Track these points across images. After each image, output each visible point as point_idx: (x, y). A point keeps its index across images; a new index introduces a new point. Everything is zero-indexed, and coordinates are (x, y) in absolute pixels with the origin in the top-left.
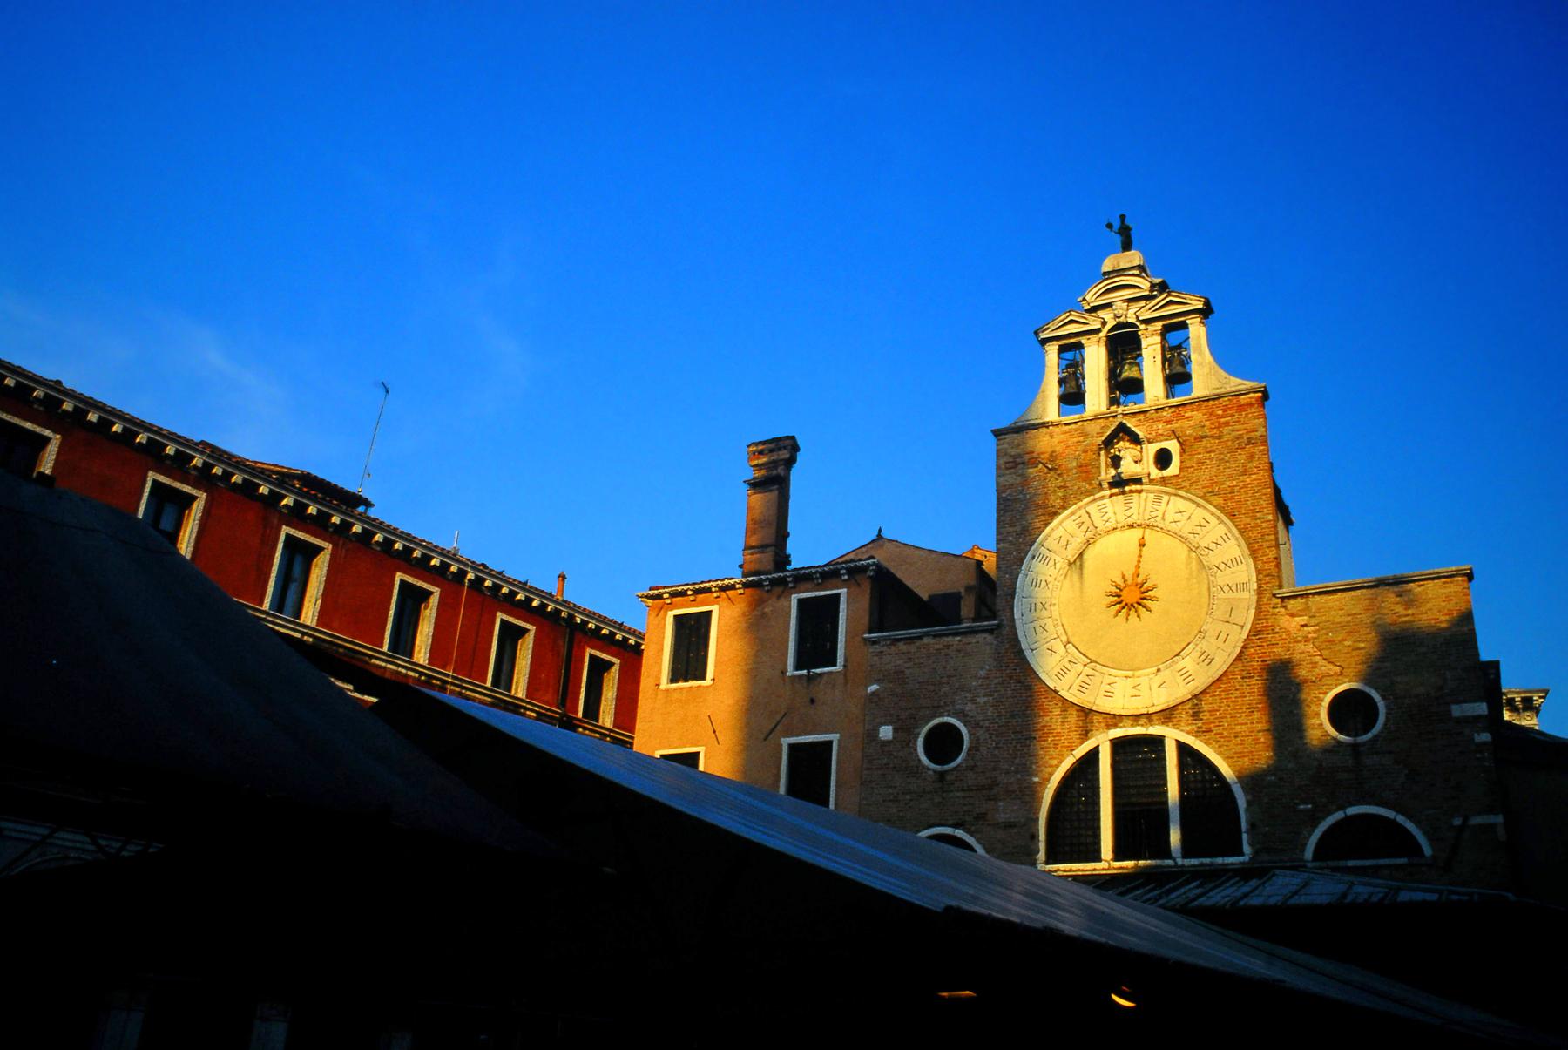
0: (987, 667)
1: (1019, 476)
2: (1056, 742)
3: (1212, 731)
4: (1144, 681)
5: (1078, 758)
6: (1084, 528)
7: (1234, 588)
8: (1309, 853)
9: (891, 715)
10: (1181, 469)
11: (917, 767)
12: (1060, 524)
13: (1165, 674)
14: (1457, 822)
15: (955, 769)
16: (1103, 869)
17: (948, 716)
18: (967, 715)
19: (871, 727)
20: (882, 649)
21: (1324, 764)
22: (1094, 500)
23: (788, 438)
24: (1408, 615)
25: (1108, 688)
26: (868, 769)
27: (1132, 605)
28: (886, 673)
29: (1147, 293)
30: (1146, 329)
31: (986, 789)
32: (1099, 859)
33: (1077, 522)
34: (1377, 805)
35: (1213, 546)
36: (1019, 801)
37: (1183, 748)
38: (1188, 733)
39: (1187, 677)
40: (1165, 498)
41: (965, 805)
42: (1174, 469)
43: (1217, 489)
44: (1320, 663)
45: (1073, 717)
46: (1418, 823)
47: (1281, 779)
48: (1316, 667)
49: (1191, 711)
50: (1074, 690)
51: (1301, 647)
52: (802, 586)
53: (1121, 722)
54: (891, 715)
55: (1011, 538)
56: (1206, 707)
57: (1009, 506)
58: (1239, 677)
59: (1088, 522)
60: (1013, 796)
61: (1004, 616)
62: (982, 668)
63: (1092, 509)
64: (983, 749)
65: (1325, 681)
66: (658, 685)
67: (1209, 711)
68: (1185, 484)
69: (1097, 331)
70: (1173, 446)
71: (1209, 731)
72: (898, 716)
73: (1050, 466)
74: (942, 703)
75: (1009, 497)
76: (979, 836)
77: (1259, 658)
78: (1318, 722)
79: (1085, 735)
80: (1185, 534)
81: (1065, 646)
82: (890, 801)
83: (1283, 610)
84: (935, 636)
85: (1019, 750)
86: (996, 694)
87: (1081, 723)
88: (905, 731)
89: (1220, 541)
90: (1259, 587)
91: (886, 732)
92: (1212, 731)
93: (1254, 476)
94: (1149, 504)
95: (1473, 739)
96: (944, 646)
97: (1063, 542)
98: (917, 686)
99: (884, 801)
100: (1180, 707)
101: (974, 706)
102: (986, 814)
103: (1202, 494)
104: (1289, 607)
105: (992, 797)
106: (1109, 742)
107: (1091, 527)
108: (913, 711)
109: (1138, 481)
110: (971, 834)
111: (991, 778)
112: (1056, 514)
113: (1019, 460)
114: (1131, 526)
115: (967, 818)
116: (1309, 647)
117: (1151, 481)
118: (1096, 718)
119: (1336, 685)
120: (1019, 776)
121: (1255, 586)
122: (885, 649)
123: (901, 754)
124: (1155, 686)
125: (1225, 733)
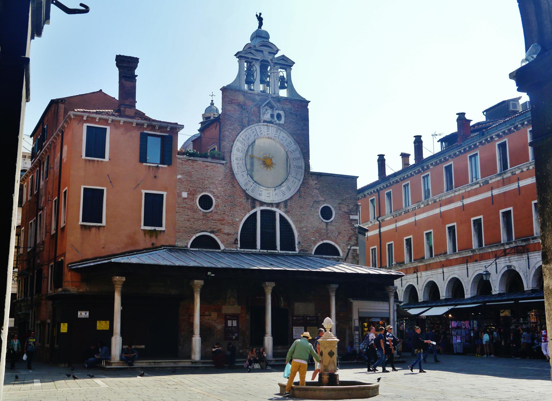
0: (221, 177)
1: (233, 107)
2: (244, 208)
3: (290, 212)
4: (271, 192)
5: (251, 214)
6: (254, 134)
7: (298, 167)
8: (313, 253)
9: (187, 188)
10: (284, 123)
11: (197, 209)
12: (247, 130)
13: (277, 191)
14: (349, 247)
15: (210, 212)
16: (258, 252)
17: (208, 192)
18: (214, 193)
19: (178, 192)
20: (182, 162)
21: (319, 227)
22: (258, 125)
23: (137, 58)
24: (342, 187)
25: (260, 192)
26: (178, 207)
27: (269, 166)
28: (184, 172)
29: (276, 52)
30: (275, 66)
31: (221, 221)
32: (256, 249)
33: (252, 131)
34: (331, 240)
35: (292, 152)
36: (232, 226)
37: (280, 215)
38: (283, 211)
39: (284, 194)
40: (279, 131)
41: (214, 225)
42: (282, 122)
43: (294, 133)
44: (320, 196)
45: (250, 201)
46: (340, 247)
47: (307, 229)
48: (318, 197)
49: (284, 205)
50: (250, 191)
51: (315, 191)
52: (150, 128)
53: (264, 204)
54: (187, 188)
55: (230, 131)
56: (289, 204)
57: (229, 118)
58: (298, 196)
59: (255, 132)
60: (230, 225)
61: (227, 158)
62: (220, 177)
63: (257, 128)
64: (220, 207)
65: (321, 202)
66: (82, 156)
67: (290, 206)
68: (285, 128)
69: (258, 60)
70: (282, 113)
71: (289, 212)
72: (189, 189)
73: (243, 107)
74: (205, 187)
75: (229, 115)
76: (219, 237)
77: (304, 191)
78: (318, 214)
79: (254, 207)
80: (285, 145)
81: (247, 175)
82: (187, 220)
83: (311, 178)
84: (203, 161)
85: (232, 209)
86: (224, 187)
87: (252, 203)
88: (192, 194)
89: (295, 151)
90: (305, 169)
91: (185, 195)
92: (290, 212)
93: (305, 132)
94: (275, 131)
95: (354, 226)
96: (206, 166)
97: (247, 137)
98: (196, 179)
99: (184, 220)
100: (282, 203)
101: (216, 191)
102: (221, 229)
103: (290, 133)
104: (313, 177)
105: (223, 224)
106: (260, 211)
107: (256, 135)
108: (195, 188)
109: (272, 123)
110: (217, 236)
111: (223, 217)
112: (245, 126)
113: (233, 101)
114: (269, 138)
115: (215, 230)
116: (317, 191)
117: (276, 124)
118: (257, 203)
119: (323, 204)
120: (232, 217)
121: (304, 168)
122: (183, 162)
123: (190, 203)
124: (274, 195)
125: (293, 214)
